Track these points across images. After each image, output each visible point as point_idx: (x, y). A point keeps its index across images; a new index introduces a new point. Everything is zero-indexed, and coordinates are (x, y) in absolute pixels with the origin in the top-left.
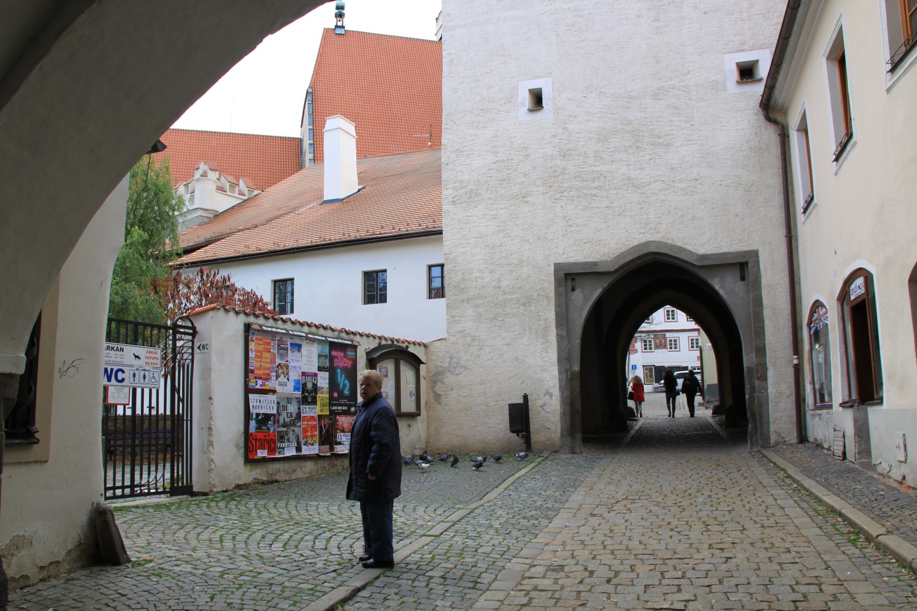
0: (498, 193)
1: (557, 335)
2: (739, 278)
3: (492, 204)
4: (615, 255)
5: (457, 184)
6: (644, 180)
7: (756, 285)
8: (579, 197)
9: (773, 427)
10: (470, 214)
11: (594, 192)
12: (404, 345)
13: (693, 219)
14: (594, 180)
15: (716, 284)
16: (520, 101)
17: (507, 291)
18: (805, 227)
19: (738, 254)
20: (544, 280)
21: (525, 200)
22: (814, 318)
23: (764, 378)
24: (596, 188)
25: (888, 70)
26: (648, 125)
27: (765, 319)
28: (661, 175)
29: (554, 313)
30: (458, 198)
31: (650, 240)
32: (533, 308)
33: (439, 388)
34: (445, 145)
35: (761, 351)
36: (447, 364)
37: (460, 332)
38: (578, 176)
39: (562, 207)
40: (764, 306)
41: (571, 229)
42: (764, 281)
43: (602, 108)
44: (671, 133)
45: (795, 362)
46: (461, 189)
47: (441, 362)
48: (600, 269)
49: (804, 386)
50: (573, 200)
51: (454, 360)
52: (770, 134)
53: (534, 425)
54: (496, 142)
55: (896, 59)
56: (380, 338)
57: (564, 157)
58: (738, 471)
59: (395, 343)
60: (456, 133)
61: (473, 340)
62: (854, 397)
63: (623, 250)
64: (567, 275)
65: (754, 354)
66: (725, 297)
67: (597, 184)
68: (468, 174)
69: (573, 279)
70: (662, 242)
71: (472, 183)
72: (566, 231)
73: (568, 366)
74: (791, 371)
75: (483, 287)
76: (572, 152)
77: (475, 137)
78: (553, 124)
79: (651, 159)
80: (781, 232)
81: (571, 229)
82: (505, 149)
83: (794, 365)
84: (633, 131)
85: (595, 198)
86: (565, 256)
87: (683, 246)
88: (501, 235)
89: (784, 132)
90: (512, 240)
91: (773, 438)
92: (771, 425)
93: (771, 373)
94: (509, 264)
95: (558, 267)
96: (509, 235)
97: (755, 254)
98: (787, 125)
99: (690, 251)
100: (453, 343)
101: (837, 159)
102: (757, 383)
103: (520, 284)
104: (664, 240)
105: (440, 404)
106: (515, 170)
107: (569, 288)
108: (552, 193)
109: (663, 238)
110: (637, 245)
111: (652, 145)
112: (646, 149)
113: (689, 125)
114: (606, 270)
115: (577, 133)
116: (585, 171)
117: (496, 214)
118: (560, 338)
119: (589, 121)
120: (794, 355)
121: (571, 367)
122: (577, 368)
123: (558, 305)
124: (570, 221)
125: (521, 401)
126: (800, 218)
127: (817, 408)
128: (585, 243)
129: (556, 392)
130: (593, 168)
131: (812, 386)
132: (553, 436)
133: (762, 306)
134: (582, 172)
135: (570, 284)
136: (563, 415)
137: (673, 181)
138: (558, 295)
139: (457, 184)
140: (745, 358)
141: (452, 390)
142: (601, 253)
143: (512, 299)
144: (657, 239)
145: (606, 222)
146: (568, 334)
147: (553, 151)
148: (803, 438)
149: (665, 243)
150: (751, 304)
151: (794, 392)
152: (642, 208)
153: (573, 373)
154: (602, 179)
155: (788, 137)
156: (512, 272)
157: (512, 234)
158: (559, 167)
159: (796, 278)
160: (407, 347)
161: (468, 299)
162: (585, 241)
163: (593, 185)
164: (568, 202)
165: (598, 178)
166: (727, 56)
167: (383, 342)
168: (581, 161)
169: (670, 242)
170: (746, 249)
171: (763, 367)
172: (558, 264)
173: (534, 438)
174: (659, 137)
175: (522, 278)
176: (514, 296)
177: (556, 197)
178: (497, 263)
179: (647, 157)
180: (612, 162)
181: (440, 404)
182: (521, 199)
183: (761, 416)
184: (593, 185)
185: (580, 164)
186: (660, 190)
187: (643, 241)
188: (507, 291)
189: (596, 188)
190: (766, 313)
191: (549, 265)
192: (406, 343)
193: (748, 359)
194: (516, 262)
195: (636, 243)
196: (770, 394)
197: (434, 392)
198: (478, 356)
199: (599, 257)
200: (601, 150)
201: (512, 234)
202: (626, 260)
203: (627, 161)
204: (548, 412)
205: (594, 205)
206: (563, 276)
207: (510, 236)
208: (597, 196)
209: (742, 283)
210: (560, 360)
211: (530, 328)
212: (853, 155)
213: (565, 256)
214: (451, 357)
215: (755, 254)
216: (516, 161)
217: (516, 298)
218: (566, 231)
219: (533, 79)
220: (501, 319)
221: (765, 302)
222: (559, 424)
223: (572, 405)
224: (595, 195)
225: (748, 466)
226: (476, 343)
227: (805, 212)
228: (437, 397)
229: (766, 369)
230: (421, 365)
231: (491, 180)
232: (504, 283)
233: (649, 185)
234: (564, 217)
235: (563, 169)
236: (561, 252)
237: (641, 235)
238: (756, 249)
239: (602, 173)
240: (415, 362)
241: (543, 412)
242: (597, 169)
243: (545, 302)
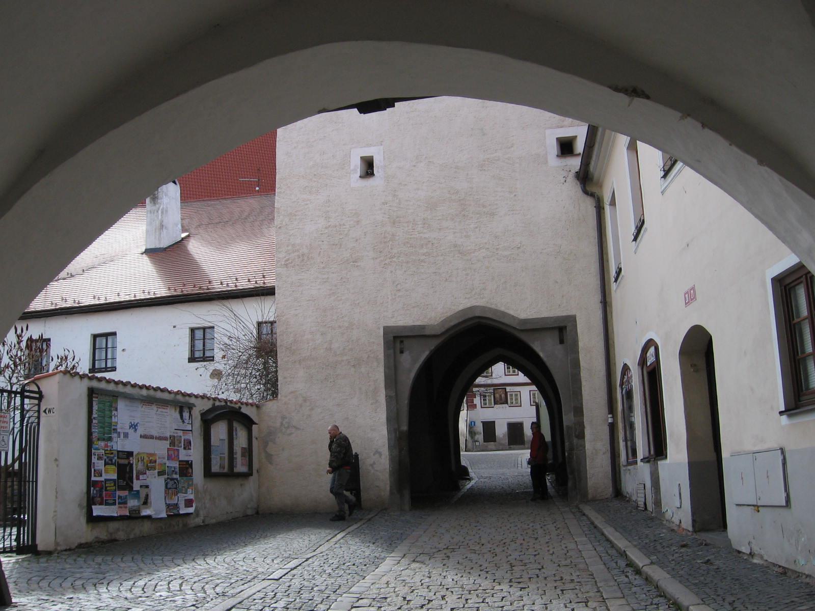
0: (329, 257)
1: (386, 397)
2: (558, 342)
3: (324, 268)
4: (442, 319)
5: (290, 248)
6: (469, 248)
8: (407, 262)
9: (590, 483)
10: (302, 277)
11: (423, 258)
12: (237, 406)
13: (515, 286)
14: (422, 246)
15: (537, 347)
16: (352, 168)
17: (338, 353)
18: (617, 293)
19: (558, 319)
20: (374, 343)
21: (356, 264)
22: (625, 380)
23: (581, 436)
24: (424, 254)
25: (662, 176)
26: (475, 195)
27: (582, 380)
28: (486, 243)
29: (383, 374)
30: (290, 261)
31: (475, 304)
32: (363, 370)
33: (271, 449)
34: (278, 209)
35: (579, 411)
36: (278, 424)
37: (292, 392)
38: (407, 243)
39: (391, 272)
40: (582, 368)
41: (400, 294)
42: (581, 344)
43: (431, 178)
44: (495, 203)
45: (610, 420)
46: (294, 252)
47: (273, 422)
48: (427, 332)
49: (619, 443)
50: (402, 266)
51: (287, 420)
52: (588, 205)
53: (362, 485)
54: (329, 207)
55: (666, 168)
56: (214, 399)
57: (394, 223)
58: (553, 523)
59: (228, 404)
60: (288, 197)
61: (305, 401)
62: (652, 452)
63: (449, 314)
64: (395, 337)
65: (572, 413)
66: (545, 359)
67: (425, 250)
68: (300, 238)
69: (402, 342)
70: (486, 307)
71: (304, 247)
72: (395, 295)
74: (606, 429)
75: (314, 348)
76: (401, 219)
77: (308, 202)
78: (384, 191)
79: (477, 228)
80: (598, 297)
81: (400, 294)
82: (337, 214)
83: (609, 423)
84: (460, 201)
85: (423, 264)
86: (393, 320)
87: (507, 311)
88: (333, 298)
89: (599, 204)
90: (343, 304)
91: (591, 493)
92: (588, 480)
93: (587, 432)
94: (340, 327)
95: (387, 330)
96: (339, 298)
97: (572, 319)
98: (603, 197)
99: (513, 316)
100: (285, 403)
101: (635, 239)
102: (575, 441)
103: (350, 347)
104: (489, 305)
105: (271, 463)
106: (347, 235)
107: (398, 351)
108: (382, 259)
109: (487, 302)
110: (462, 310)
111: (477, 214)
112: (472, 218)
113: (512, 196)
114: (433, 333)
115: (407, 201)
116: (414, 238)
117: (328, 278)
118: (389, 398)
119: (418, 189)
120: (609, 414)
122: (405, 428)
123: (387, 367)
124: (399, 286)
126: (614, 286)
127: (629, 464)
128: (414, 307)
129: (385, 451)
130: (421, 235)
131: (624, 443)
132: (383, 494)
133: (580, 367)
134: (411, 238)
136: (392, 473)
137: (497, 249)
138: (386, 356)
139: (290, 248)
140: (563, 416)
141: (283, 450)
142: (429, 317)
143: (342, 361)
144: (482, 304)
145: (433, 287)
146: (397, 395)
147: (383, 217)
148: (618, 492)
149: (490, 308)
150: (569, 366)
151: (609, 448)
152: (467, 275)
154: (430, 246)
155: (603, 209)
156: (343, 334)
157: (343, 298)
158: (388, 233)
159: (611, 342)
160: (240, 408)
161: (300, 361)
162: (414, 305)
163: (422, 251)
164: (397, 267)
165: (427, 245)
166: (548, 132)
167: (217, 403)
168: (410, 227)
169: (493, 306)
170: (564, 314)
172: (387, 327)
173: (364, 495)
174: (484, 206)
175: (353, 341)
176: (345, 358)
177: (386, 262)
178: (328, 326)
179: (472, 226)
180: (440, 229)
181: (271, 463)
182: (352, 263)
184: (422, 251)
185: (409, 231)
186: (484, 257)
187: (469, 305)
188: (338, 353)
189: (424, 254)
190: (584, 374)
191: (379, 328)
192: (239, 404)
193: (568, 419)
194: (346, 324)
195: (461, 307)
196: (587, 451)
197: (266, 452)
198: (310, 416)
199: (426, 320)
200: (429, 217)
201: (343, 298)
202: (452, 324)
203: (453, 229)
204: (377, 471)
205: (423, 271)
206: (392, 338)
207: (341, 300)
208: (425, 262)
209: (560, 347)
210: (389, 420)
211: (360, 389)
212: (645, 236)
213: (393, 320)
214: (283, 418)
215: (572, 319)
216: (348, 227)
217: (347, 360)
218: (395, 295)
219: (365, 147)
220: (331, 380)
221: (582, 363)
222: (388, 482)
224: (423, 261)
225: (564, 518)
226: (308, 404)
227: (616, 281)
228: (269, 457)
229: (584, 427)
230: (254, 426)
231: (323, 244)
232: (335, 346)
233: (474, 252)
234: (394, 282)
235: (393, 235)
236: (390, 316)
237: (467, 300)
238: (574, 314)
239: (430, 240)
240: (248, 422)
241: (372, 471)
242: (426, 236)
243: (375, 364)
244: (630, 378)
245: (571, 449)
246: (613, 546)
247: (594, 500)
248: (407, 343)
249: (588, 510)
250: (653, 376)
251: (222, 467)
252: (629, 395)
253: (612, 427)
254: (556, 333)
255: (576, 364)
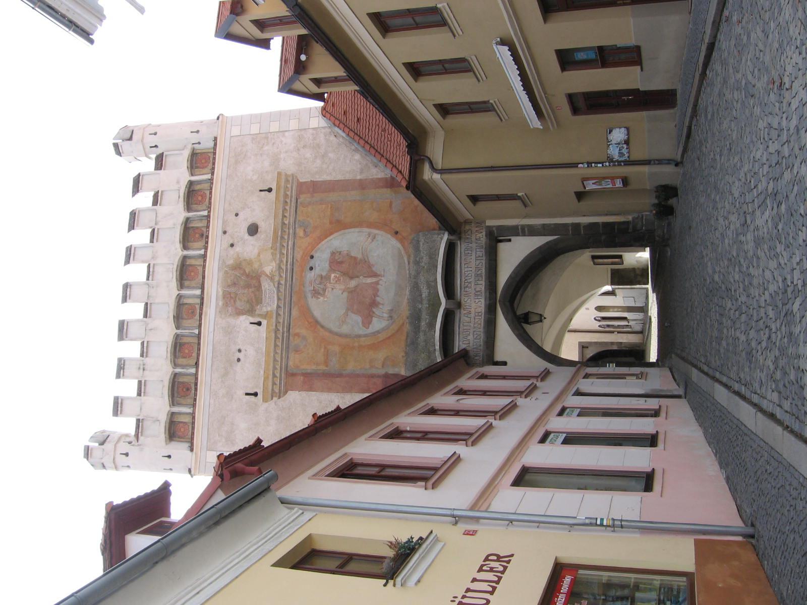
7: (590, 343)
9: (638, 342)
15: (588, 356)
23: (621, 343)
35: (612, 343)
91: (641, 341)
97: (580, 343)
102: (623, 345)
190: (599, 341)
215: (580, 343)
221: (596, 341)
244: (604, 325)
250: (604, 318)
252: (608, 326)
253: (619, 332)
254: (584, 349)
255: (596, 343)
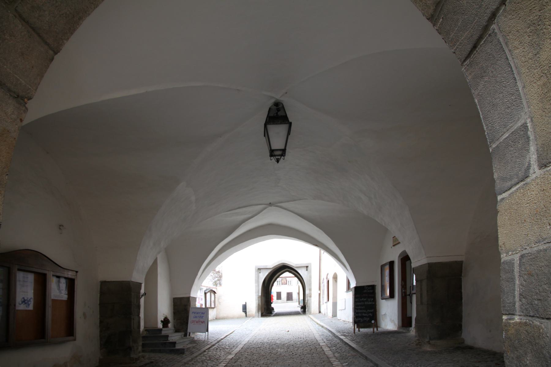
23: (310, 297)
35: (310, 290)
45: (319, 292)
53: (247, 311)
56: (207, 287)
69: (260, 270)
73: (258, 294)
102: (309, 298)
107: (259, 272)
121: (259, 294)
122: (260, 294)
125: (245, 304)
135: (259, 271)
153: (259, 296)
167: (208, 288)
171: (310, 294)
173: (247, 314)
183: (309, 307)
223: (259, 304)
228: (220, 303)
240: (215, 292)
245: (308, 300)
246: (314, 321)
247: (313, 314)
248: (261, 270)
249: (311, 316)
251: (209, 306)
253: (320, 294)
